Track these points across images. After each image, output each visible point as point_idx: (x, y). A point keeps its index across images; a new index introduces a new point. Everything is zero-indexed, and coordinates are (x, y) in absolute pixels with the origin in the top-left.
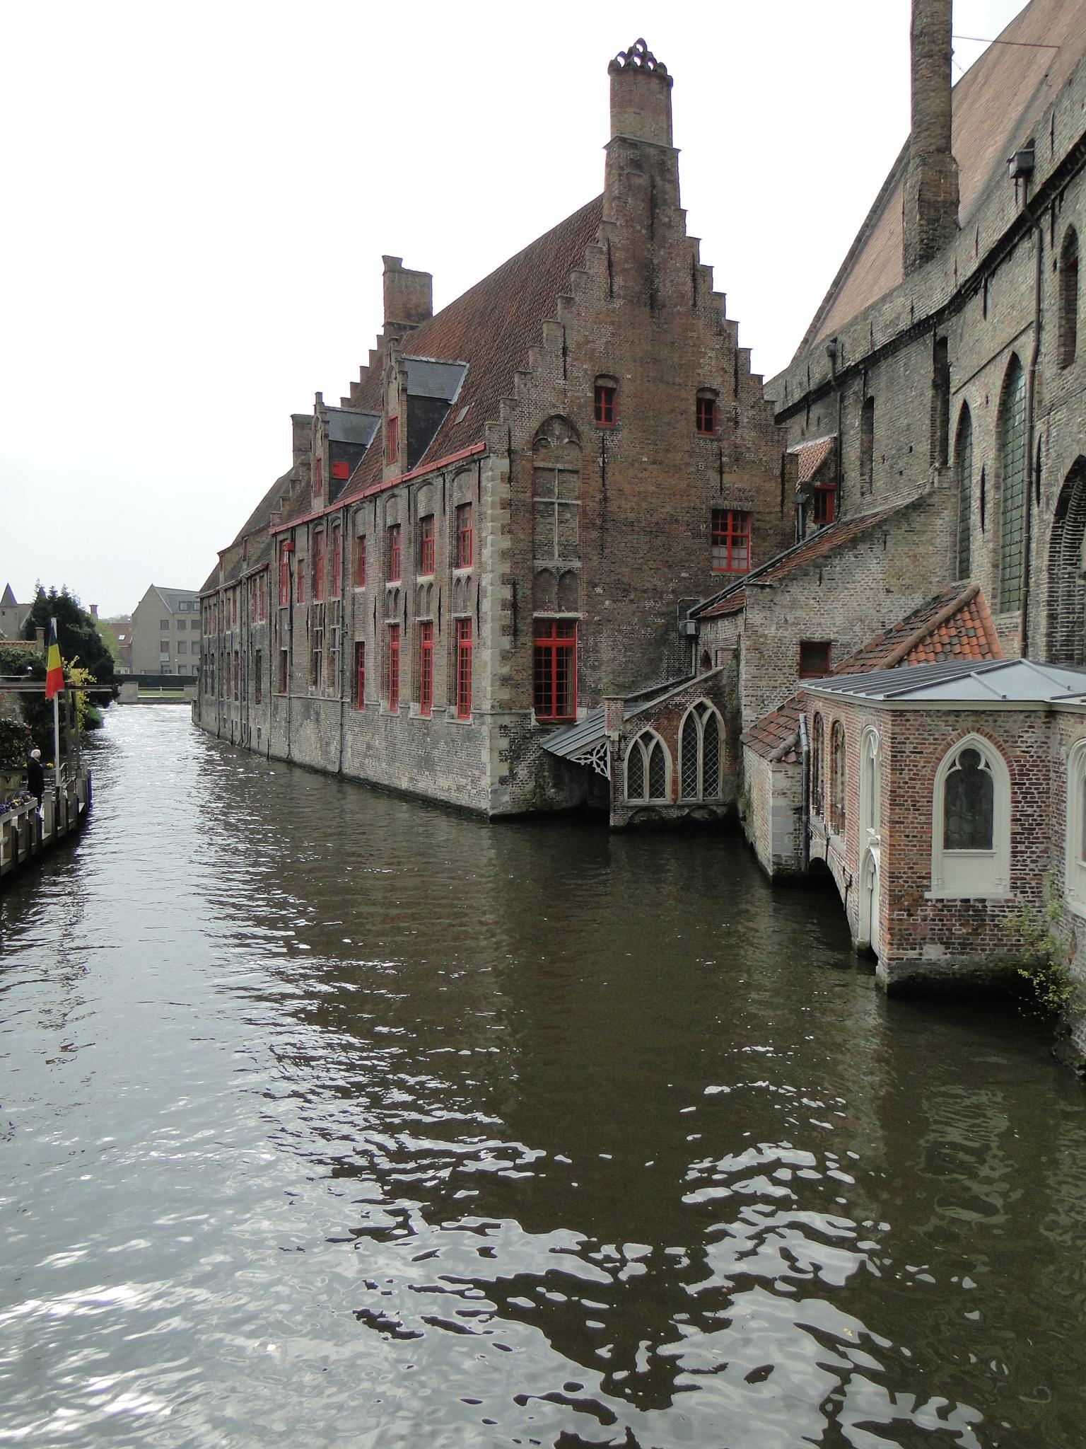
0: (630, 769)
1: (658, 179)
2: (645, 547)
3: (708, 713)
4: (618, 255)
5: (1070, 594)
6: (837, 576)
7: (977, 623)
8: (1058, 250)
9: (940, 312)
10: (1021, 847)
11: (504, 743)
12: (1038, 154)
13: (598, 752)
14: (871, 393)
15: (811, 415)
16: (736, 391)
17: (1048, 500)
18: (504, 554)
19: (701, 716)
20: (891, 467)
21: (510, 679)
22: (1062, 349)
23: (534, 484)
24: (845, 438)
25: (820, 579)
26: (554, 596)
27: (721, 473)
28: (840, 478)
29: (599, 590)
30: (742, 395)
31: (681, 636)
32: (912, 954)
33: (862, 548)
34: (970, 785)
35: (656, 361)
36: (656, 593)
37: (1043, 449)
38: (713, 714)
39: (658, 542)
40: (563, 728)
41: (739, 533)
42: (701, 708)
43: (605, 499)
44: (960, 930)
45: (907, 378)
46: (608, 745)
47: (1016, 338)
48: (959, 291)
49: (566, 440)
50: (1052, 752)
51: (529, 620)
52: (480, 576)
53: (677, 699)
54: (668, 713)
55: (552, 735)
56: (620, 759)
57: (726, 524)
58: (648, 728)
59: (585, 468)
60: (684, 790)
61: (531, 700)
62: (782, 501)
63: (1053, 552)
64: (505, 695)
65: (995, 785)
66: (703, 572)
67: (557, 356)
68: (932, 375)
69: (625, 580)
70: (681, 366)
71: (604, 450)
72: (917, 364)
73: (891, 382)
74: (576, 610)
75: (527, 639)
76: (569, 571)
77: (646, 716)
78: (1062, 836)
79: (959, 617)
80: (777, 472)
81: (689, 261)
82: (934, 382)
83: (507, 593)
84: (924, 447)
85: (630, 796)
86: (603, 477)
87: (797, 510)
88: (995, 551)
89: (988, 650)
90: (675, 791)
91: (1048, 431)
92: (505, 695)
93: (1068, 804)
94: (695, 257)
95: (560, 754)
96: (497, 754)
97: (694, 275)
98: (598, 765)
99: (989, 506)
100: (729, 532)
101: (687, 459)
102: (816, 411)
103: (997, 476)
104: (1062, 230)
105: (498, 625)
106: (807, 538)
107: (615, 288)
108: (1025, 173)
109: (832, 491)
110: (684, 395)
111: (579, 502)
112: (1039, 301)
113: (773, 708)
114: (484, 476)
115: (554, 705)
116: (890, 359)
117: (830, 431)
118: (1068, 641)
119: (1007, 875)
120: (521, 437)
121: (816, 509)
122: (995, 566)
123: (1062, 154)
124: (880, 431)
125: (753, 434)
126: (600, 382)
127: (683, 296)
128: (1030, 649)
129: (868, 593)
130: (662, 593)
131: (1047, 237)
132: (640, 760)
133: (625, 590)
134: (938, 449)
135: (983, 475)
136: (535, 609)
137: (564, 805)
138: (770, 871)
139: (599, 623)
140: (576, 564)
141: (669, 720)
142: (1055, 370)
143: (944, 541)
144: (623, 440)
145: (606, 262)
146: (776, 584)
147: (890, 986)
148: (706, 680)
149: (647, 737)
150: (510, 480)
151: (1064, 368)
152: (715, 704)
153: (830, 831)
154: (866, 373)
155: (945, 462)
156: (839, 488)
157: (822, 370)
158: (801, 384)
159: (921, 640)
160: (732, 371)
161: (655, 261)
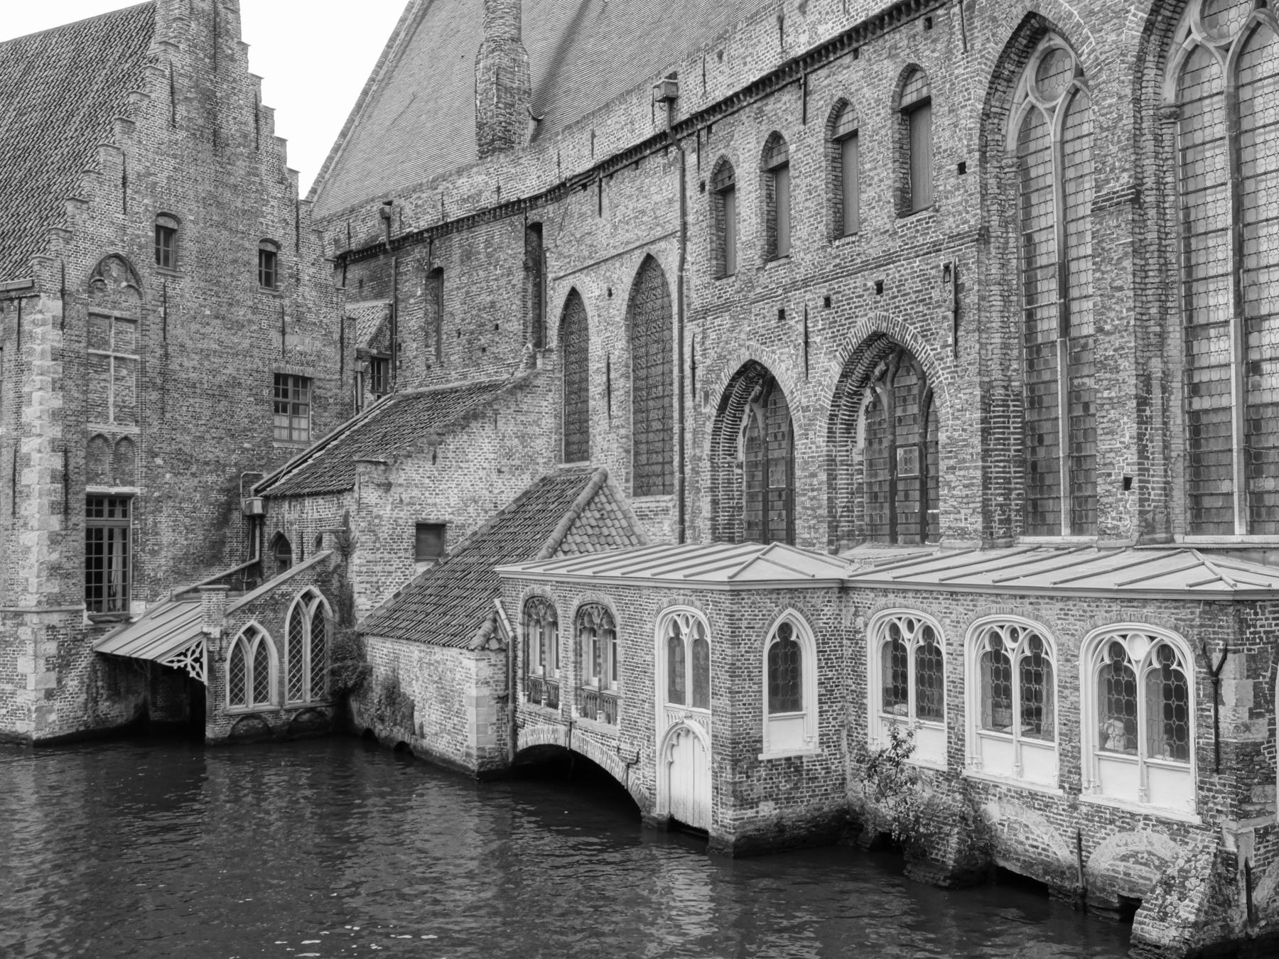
0: (232, 671)
1: (220, 6)
2: (209, 413)
3: (315, 603)
4: (182, 82)
5: (729, 482)
6: (450, 455)
7: (614, 505)
8: (707, 175)
9: (536, 198)
10: (825, 707)
11: (51, 648)
12: (681, 85)
13: (194, 652)
14: (437, 263)
15: (349, 275)
16: (297, 245)
17: (707, 395)
18: (56, 415)
19: (307, 605)
20: (469, 342)
21: (60, 568)
22: (714, 262)
23: (89, 332)
24: (401, 306)
25: (434, 457)
26: (107, 467)
27: (283, 333)
28: (395, 347)
29: (159, 461)
30: (303, 250)
31: (244, 516)
32: (750, 813)
33: (475, 425)
34: (785, 657)
35: (219, 205)
36: (219, 466)
37: (697, 347)
38: (321, 605)
39: (221, 407)
40: (118, 627)
41: (301, 401)
42: (308, 597)
43: (166, 355)
44: (785, 786)
45: (489, 256)
46: (204, 644)
47: (652, 243)
48: (563, 184)
49: (124, 284)
50: (846, 623)
51: (82, 496)
52: (17, 441)
53: (284, 587)
54: (274, 603)
55: (107, 635)
56: (222, 660)
57: (288, 389)
58: (252, 622)
59: (145, 317)
60: (290, 691)
61: (83, 594)
62: (342, 368)
63: (715, 444)
64: (54, 587)
65: (803, 654)
66: (266, 443)
67: (116, 186)
68: (522, 257)
69: (187, 450)
70: (244, 212)
71: (165, 299)
72: (507, 243)
73: (468, 255)
74: (132, 484)
75: (80, 519)
76: (126, 438)
77: (250, 608)
78: (862, 694)
79: (597, 500)
80: (336, 337)
81: (251, 95)
82: (525, 264)
83: (57, 462)
84: (515, 326)
85: (232, 701)
86: (164, 330)
87: (356, 378)
88: (627, 437)
89: (629, 532)
90: (281, 695)
91: (704, 332)
92: (54, 587)
93: (869, 666)
94: (257, 97)
95: (148, 655)
96: (42, 662)
97: (256, 115)
98: (193, 668)
99: (618, 395)
100: (291, 399)
101: (250, 316)
102: (355, 272)
103: (627, 366)
104: (712, 159)
105: (46, 501)
106: (366, 410)
107: (178, 117)
108: (671, 101)
109: (386, 360)
110: (247, 245)
111: (137, 357)
112: (684, 213)
113: (388, 595)
114: (27, 319)
115: (105, 598)
116: (465, 234)
117: (380, 295)
118: (730, 525)
119: (816, 732)
120: (76, 276)
121: (373, 378)
122: (628, 451)
123: (719, 95)
124: (454, 305)
125: (314, 293)
126: (161, 221)
127: (245, 136)
128: (688, 533)
129: (482, 473)
130: (225, 466)
131: (692, 159)
132: (241, 660)
133: (186, 461)
134: (530, 330)
135: (608, 364)
136: (89, 481)
137: (120, 721)
138: (473, 765)
139: (158, 500)
140: (133, 430)
141: (275, 611)
142: (707, 279)
143: (549, 422)
144: (186, 288)
145: (168, 88)
146: (390, 461)
147: (735, 845)
148: (312, 567)
149: (251, 632)
150: (62, 326)
151: (718, 279)
152: (323, 592)
153: (575, 715)
154: (431, 242)
155: (539, 343)
156: (393, 357)
157: (365, 231)
158: (337, 241)
159: (572, 522)
160: (294, 223)
161: (218, 94)
